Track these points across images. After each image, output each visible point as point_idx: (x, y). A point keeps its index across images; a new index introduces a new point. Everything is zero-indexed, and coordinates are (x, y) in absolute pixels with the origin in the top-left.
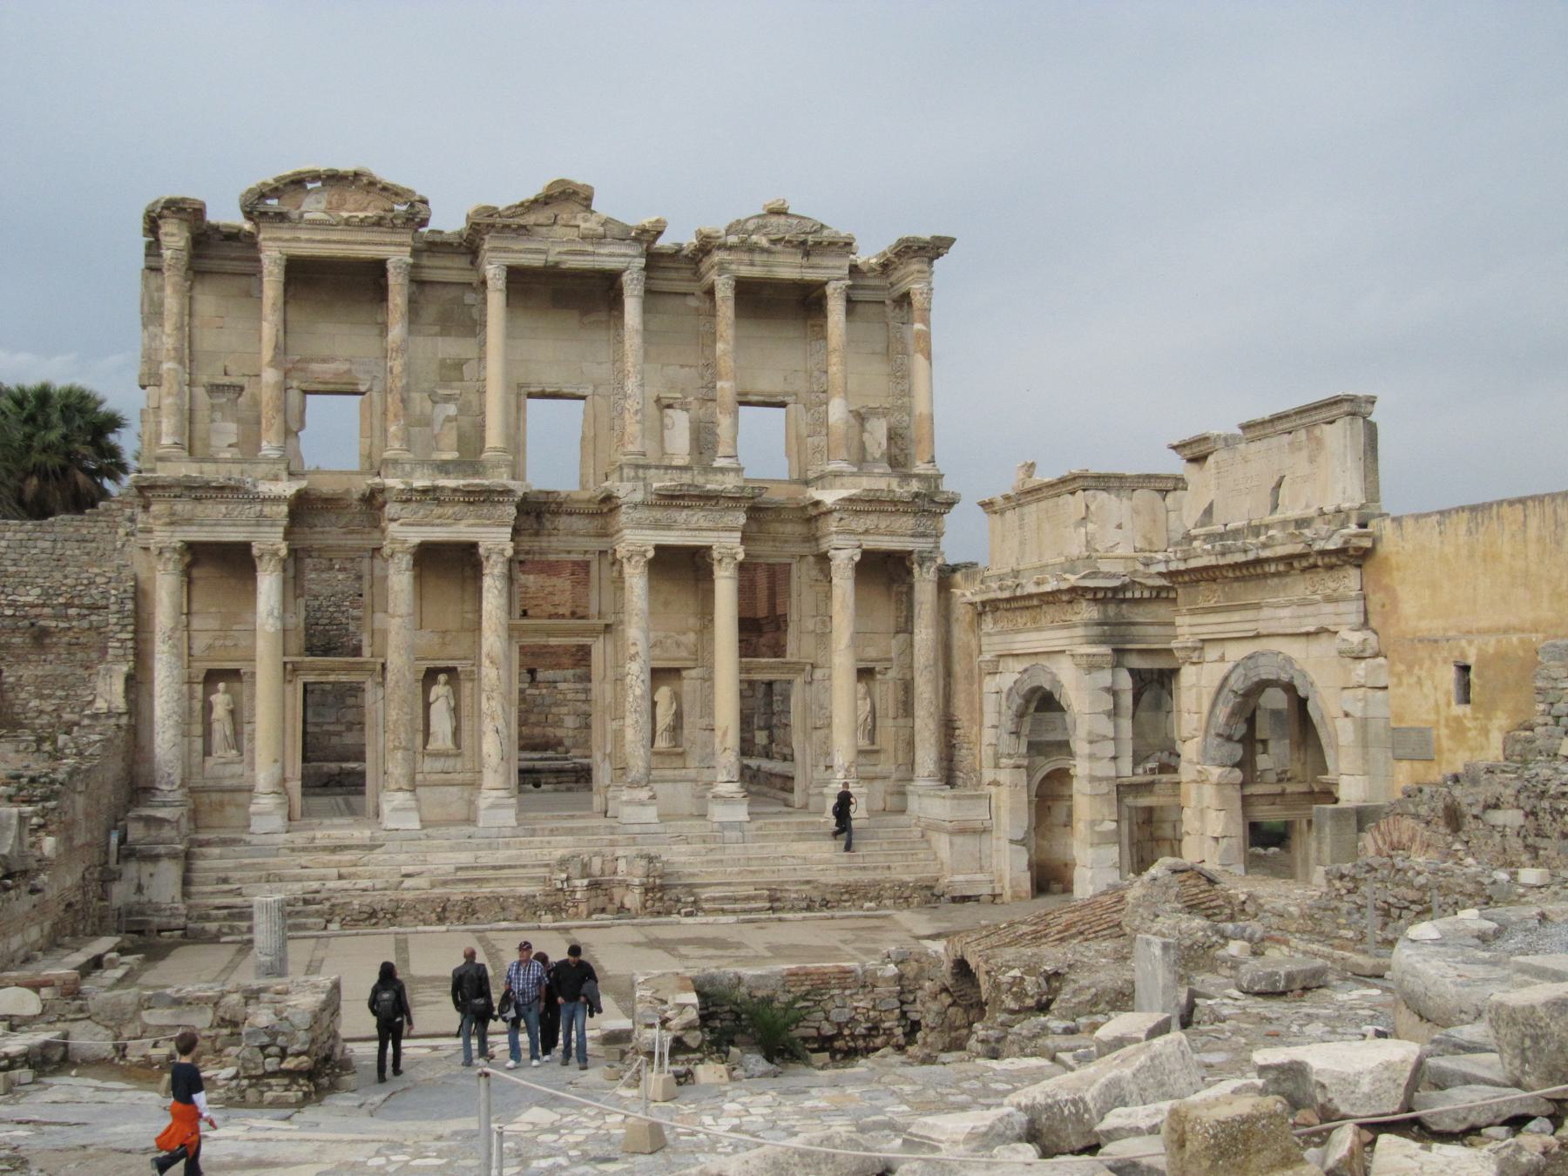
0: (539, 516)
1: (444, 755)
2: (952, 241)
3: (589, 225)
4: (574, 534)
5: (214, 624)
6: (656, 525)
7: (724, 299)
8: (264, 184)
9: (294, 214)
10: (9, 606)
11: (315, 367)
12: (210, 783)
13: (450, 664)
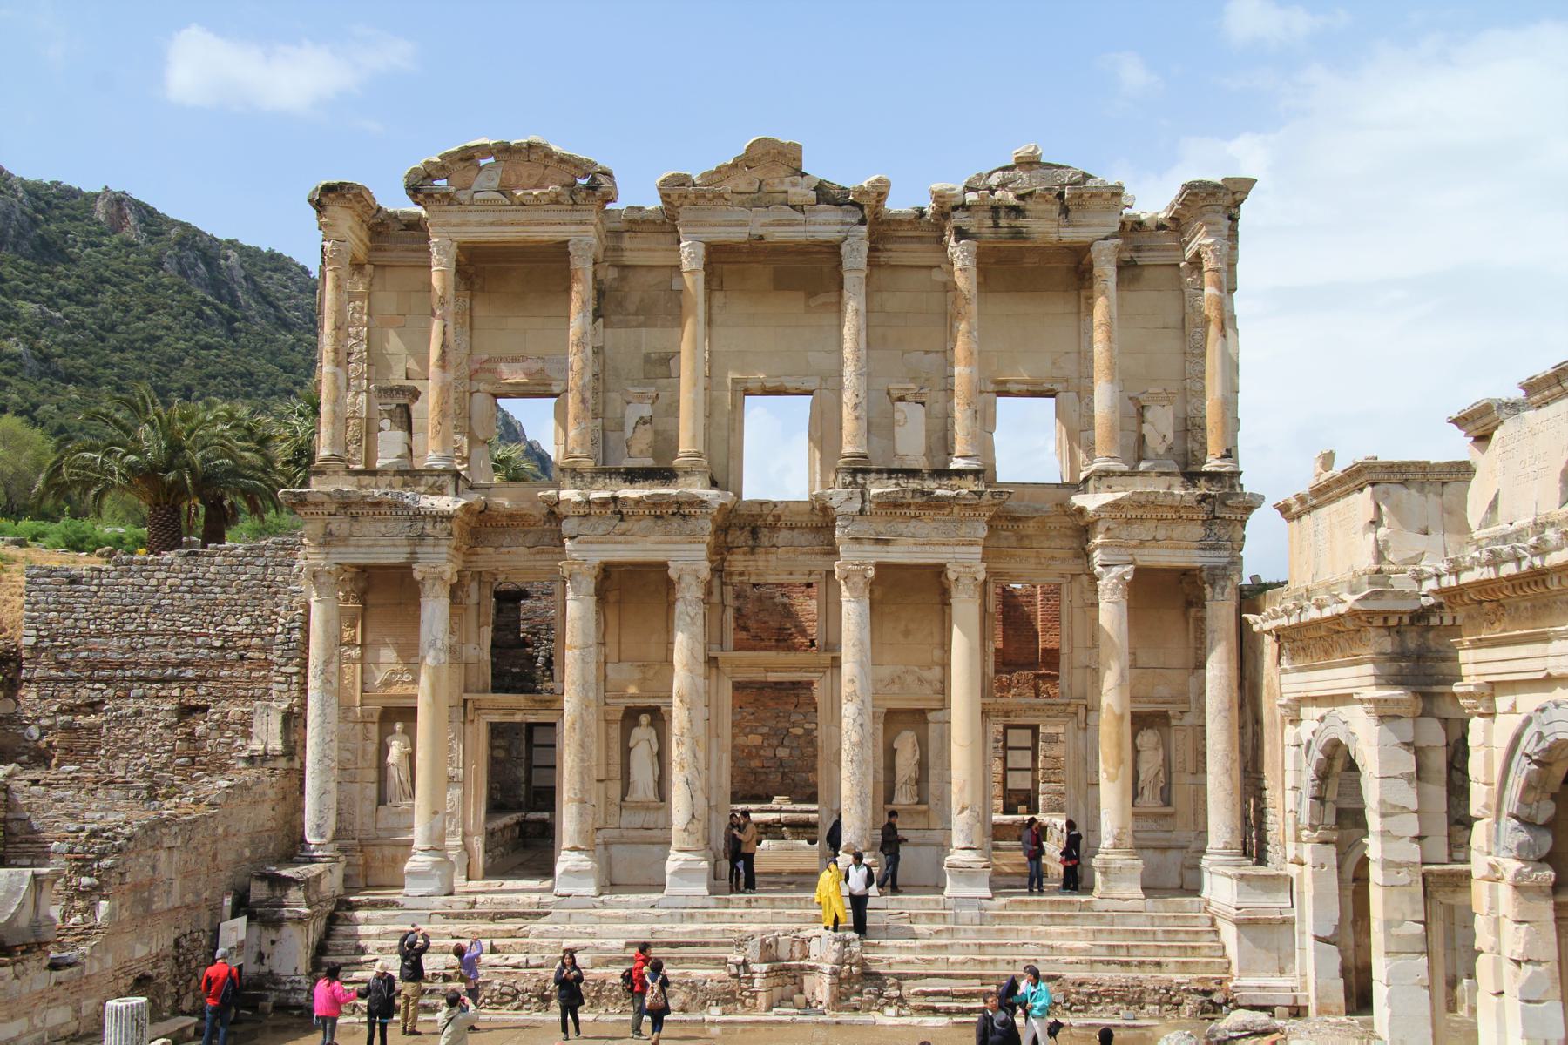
0: (754, 532)
1: (644, 807)
2: (1253, 182)
3: (802, 192)
6: (879, 541)
7: (963, 269)
8: (428, 163)
9: (463, 196)
10: (218, 636)
13: (653, 702)
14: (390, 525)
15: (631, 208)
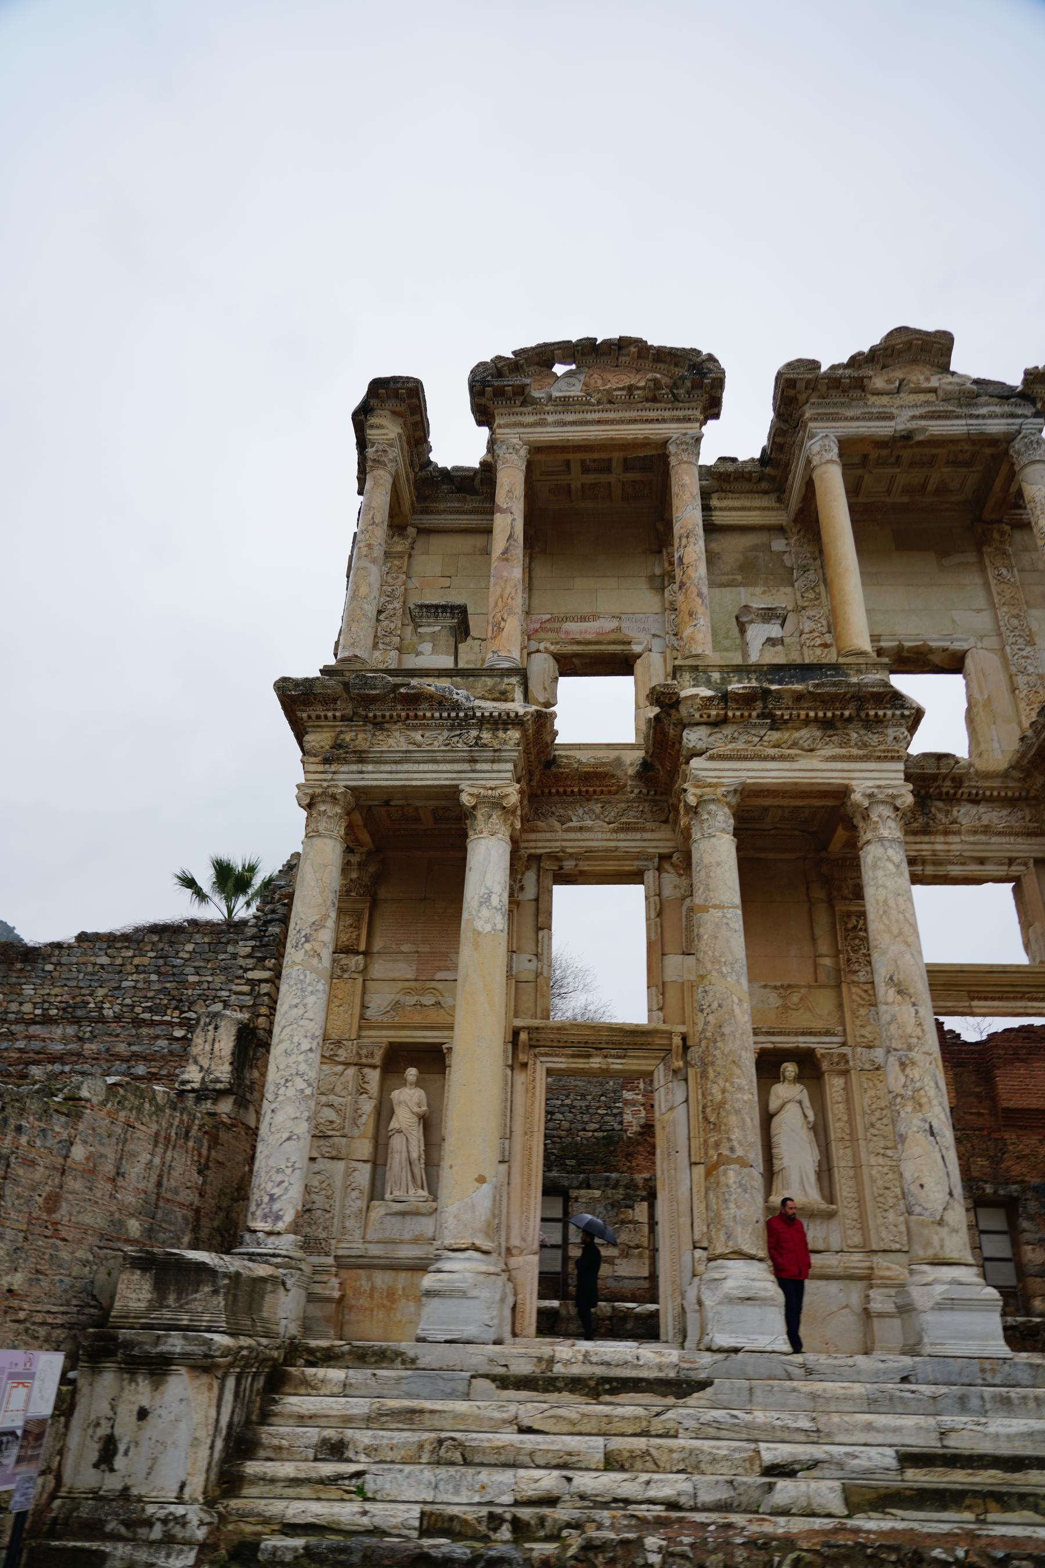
4: (986, 830)
5: (405, 970)
8: (499, 358)
11: (569, 626)
12: (375, 1250)
14: (427, 734)
15: (722, 459)
